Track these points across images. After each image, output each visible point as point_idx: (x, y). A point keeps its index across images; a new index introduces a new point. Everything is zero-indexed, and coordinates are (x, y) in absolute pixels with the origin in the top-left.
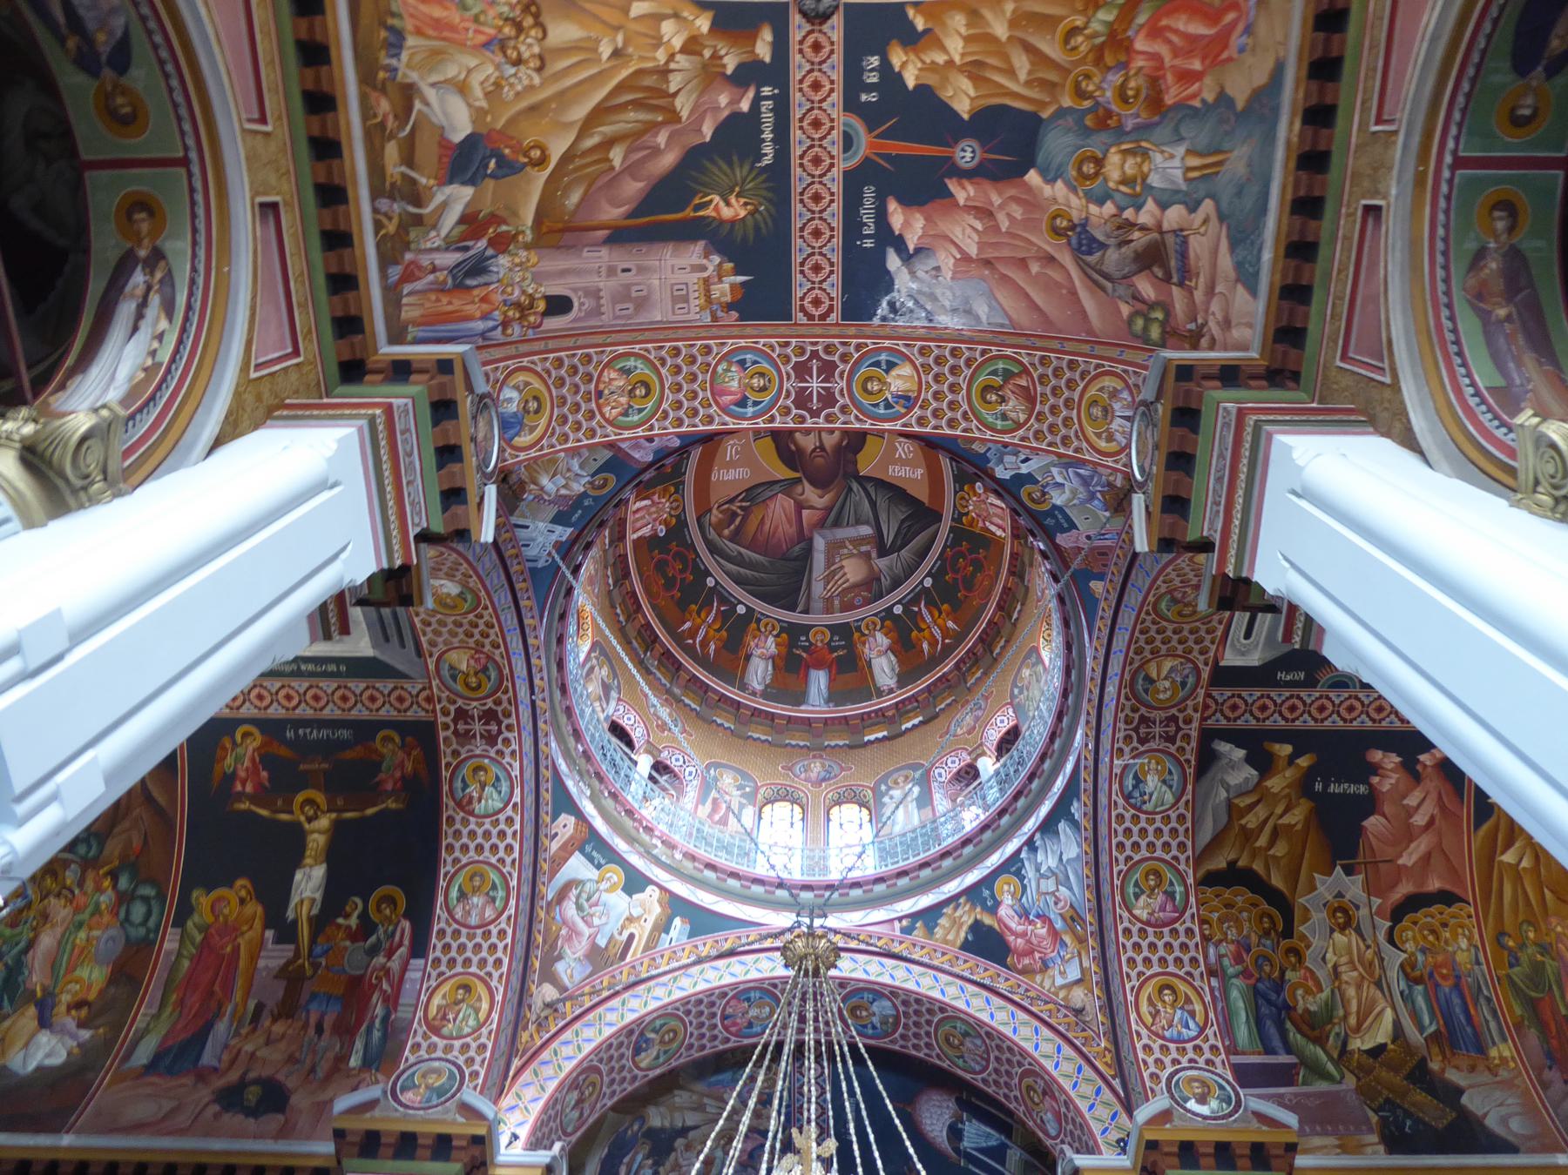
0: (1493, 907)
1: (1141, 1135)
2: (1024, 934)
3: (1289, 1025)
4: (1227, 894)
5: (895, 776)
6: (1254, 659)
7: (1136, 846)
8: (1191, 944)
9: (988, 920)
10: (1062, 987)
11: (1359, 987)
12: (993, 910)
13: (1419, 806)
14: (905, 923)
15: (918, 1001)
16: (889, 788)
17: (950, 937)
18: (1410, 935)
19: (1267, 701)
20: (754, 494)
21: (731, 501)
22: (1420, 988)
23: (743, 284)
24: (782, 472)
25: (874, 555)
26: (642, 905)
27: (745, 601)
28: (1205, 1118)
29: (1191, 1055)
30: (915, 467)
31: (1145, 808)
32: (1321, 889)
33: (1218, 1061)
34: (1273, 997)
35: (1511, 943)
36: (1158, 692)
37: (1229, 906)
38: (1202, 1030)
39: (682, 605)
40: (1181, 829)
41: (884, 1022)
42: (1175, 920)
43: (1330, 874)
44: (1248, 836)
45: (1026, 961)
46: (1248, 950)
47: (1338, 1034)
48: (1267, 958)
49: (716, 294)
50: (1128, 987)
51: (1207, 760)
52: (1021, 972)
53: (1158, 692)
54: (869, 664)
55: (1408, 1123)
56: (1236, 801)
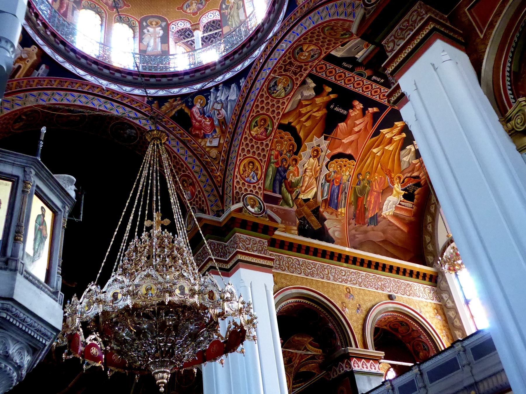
1: (230, 214)
2: (200, 122)
3: (283, 185)
4: (283, 133)
5: (151, 19)
9: (186, 110)
10: (209, 147)
11: (310, 178)
12: (191, 107)
13: (359, 124)
16: (148, 26)
18: (333, 166)
22: (328, 184)
26: (28, 53)
28: (253, 213)
29: (252, 189)
31: (273, 95)
32: (314, 142)
33: (260, 193)
34: (282, 173)
35: (361, 178)
36: (302, 55)
38: (258, 180)
43: (319, 138)
44: (300, 115)
45: (197, 132)
46: (281, 155)
47: (297, 192)
48: (286, 160)
50: (239, 158)
55: (307, 226)
56: (303, 102)
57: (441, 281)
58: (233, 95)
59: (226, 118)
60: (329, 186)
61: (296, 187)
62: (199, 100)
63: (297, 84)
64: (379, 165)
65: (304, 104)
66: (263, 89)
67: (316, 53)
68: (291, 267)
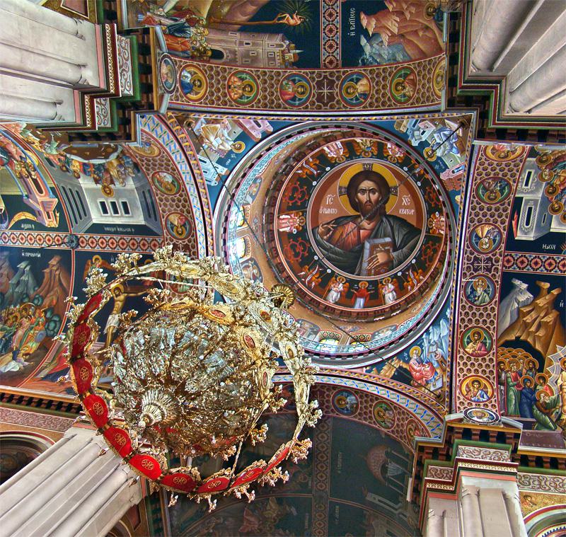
3: (535, 407)
4: (514, 351)
6: (531, 237)
7: (470, 320)
8: (491, 365)
9: (405, 366)
12: (407, 362)
14: (368, 368)
15: (367, 396)
17: (387, 374)
19: (538, 260)
20: (340, 221)
21: (328, 224)
23: (298, 54)
24: (352, 212)
25: (391, 251)
27: (331, 267)
30: (411, 209)
31: (475, 303)
32: (559, 352)
36: (483, 244)
37: (514, 356)
38: (489, 399)
39: (302, 265)
40: (492, 314)
41: (352, 407)
42: (485, 355)
44: (527, 326)
46: (521, 376)
47: (557, 412)
49: (287, 58)
50: (458, 379)
51: (507, 289)
52: (416, 387)
53: (483, 244)
54: (384, 296)
56: (522, 309)
58: (444, 329)
59: (444, 356)
61: (555, 407)
62: (415, 351)
63: (497, 282)
65: (525, 311)
66: (462, 300)
67: (495, 233)
68: (560, 487)
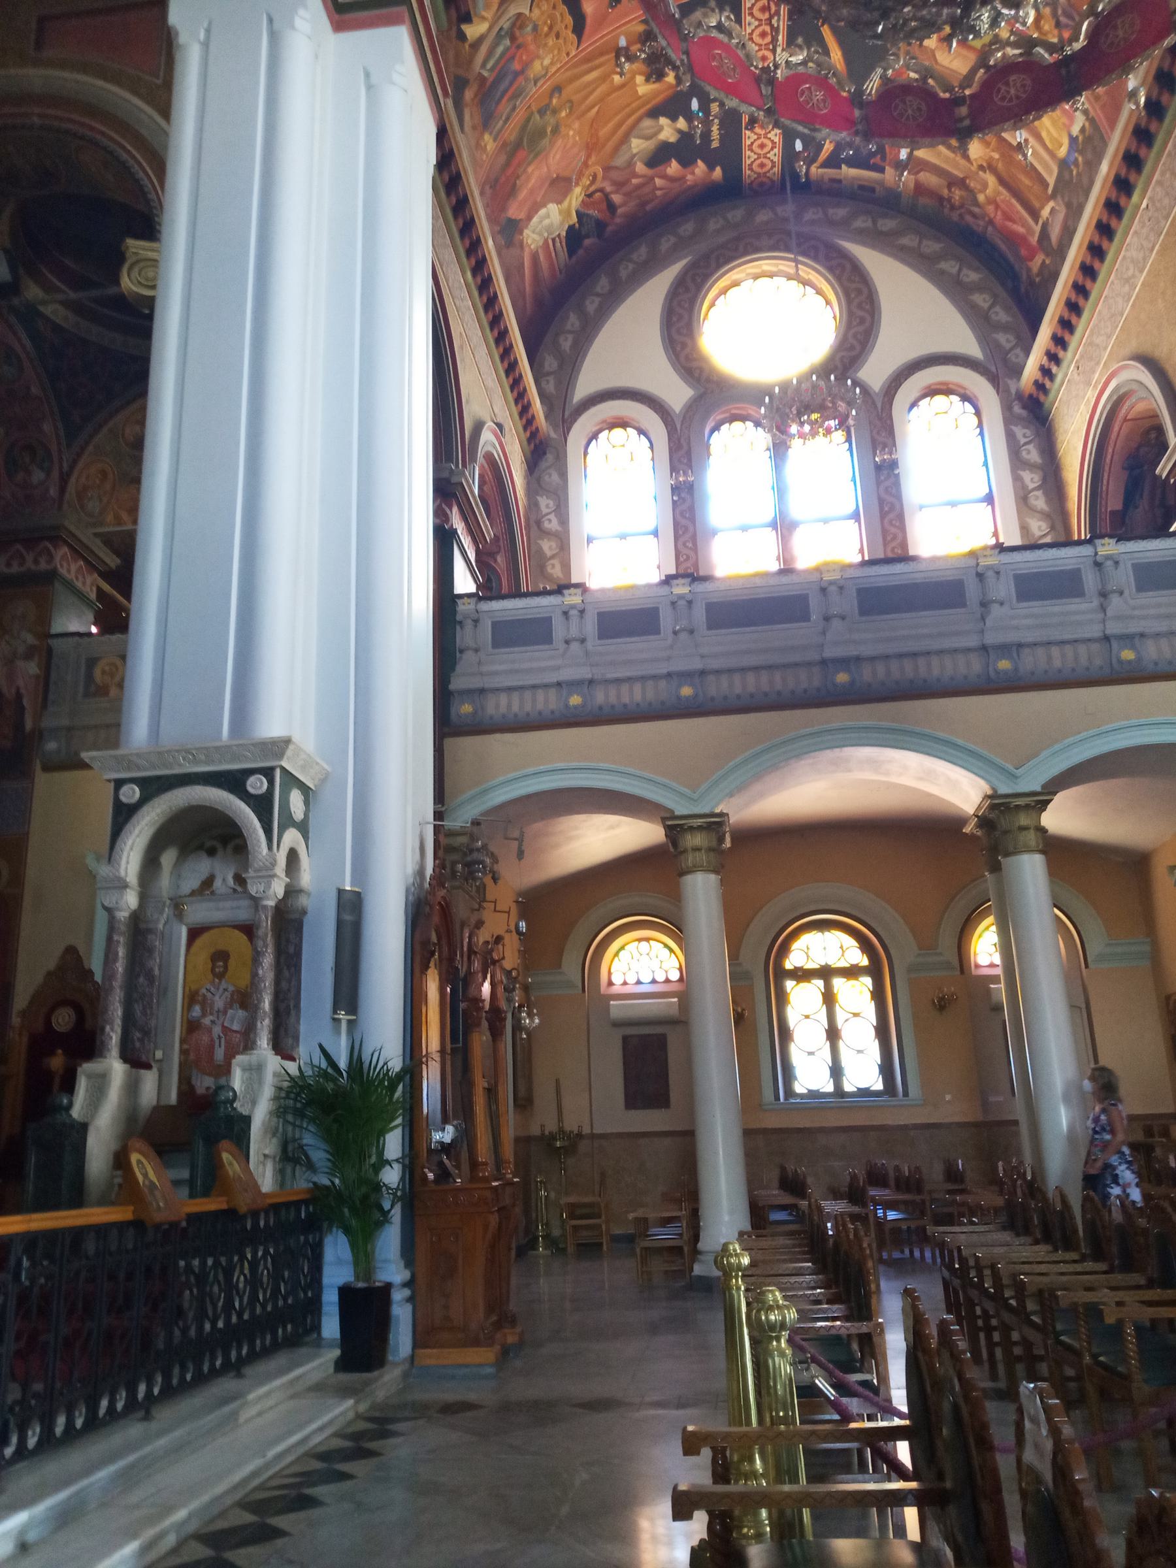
0: (576, 71)
35: (554, 101)
57: (549, 467)
60: (507, 50)
64: (596, 109)
